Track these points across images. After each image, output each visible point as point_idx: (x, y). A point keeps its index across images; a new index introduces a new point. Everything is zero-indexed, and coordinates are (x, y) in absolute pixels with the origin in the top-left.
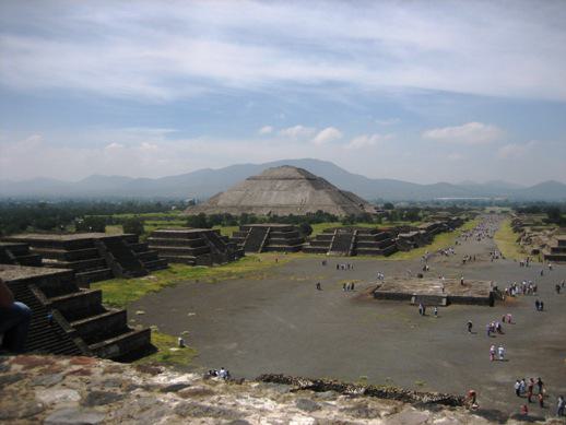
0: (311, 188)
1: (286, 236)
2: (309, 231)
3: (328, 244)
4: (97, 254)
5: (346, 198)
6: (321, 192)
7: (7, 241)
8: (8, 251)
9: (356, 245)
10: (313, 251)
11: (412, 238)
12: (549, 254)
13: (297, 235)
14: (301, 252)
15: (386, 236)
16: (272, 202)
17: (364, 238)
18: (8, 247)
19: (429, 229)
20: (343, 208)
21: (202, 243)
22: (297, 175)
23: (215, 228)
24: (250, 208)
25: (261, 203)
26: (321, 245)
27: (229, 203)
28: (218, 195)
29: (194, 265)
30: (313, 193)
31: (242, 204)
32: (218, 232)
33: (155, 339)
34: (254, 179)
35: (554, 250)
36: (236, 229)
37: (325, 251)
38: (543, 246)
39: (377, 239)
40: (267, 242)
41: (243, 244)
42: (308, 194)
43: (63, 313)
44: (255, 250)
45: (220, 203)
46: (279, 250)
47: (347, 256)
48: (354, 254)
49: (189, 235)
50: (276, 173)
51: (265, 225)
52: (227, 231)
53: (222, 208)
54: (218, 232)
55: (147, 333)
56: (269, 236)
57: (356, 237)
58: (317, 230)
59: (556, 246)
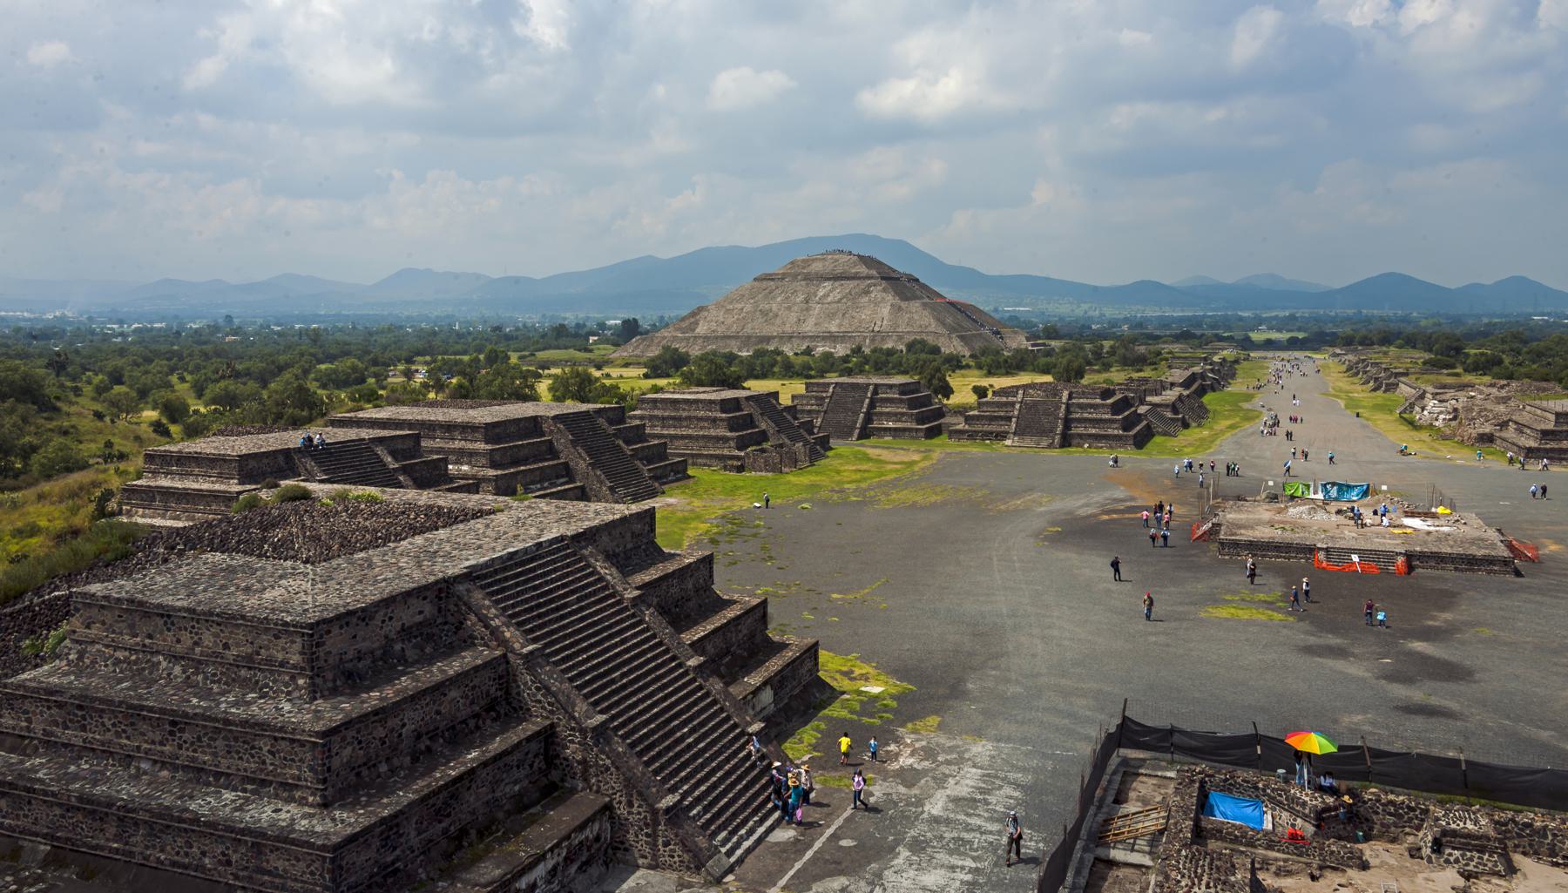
0: (890, 298)
1: (912, 404)
2: (947, 391)
3: (1009, 419)
4: (552, 452)
5: (963, 315)
6: (915, 306)
7: (360, 423)
8: (379, 450)
9: (1068, 423)
10: (972, 436)
11: (1174, 408)
12: (1532, 444)
13: (927, 401)
14: (944, 437)
15: (1125, 403)
16: (809, 327)
17: (1082, 407)
18: (380, 440)
19: (1187, 384)
20: (962, 338)
21: (749, 421)
22: (863, 270)
23: (757, 386)
24: (768, 339)
25: (788, 329)
26: (987, 423)
27: (721, 330)
28: (693, 314)
29: (740, 469)
30: (897, 309)
31: (748, 330)
32: (775, 395)
33: (830, 665)
34: (768, 278)
35: (1546, 434)
36: (798, 387)
37: (1001, 436)
38: (1503, 425)
39: (1117, 408)
40: (869, 418)
41: (818, 422)
42: (885, 311)
43: (663, 610)
44: (845, 434)
45: (701, 329)
46: (896, 432)
47: (1050, 446)
48: (1066, 441)
49: (725, 405)
50: (817, 267)
51: (860, 380)
52: (788, 391)
53: (706, 338)
54: (775, 395)
55: (812, 651)
56: (872, 405)
57: (1068, 405)
58: (963, 389)
59: (1551, 426)
